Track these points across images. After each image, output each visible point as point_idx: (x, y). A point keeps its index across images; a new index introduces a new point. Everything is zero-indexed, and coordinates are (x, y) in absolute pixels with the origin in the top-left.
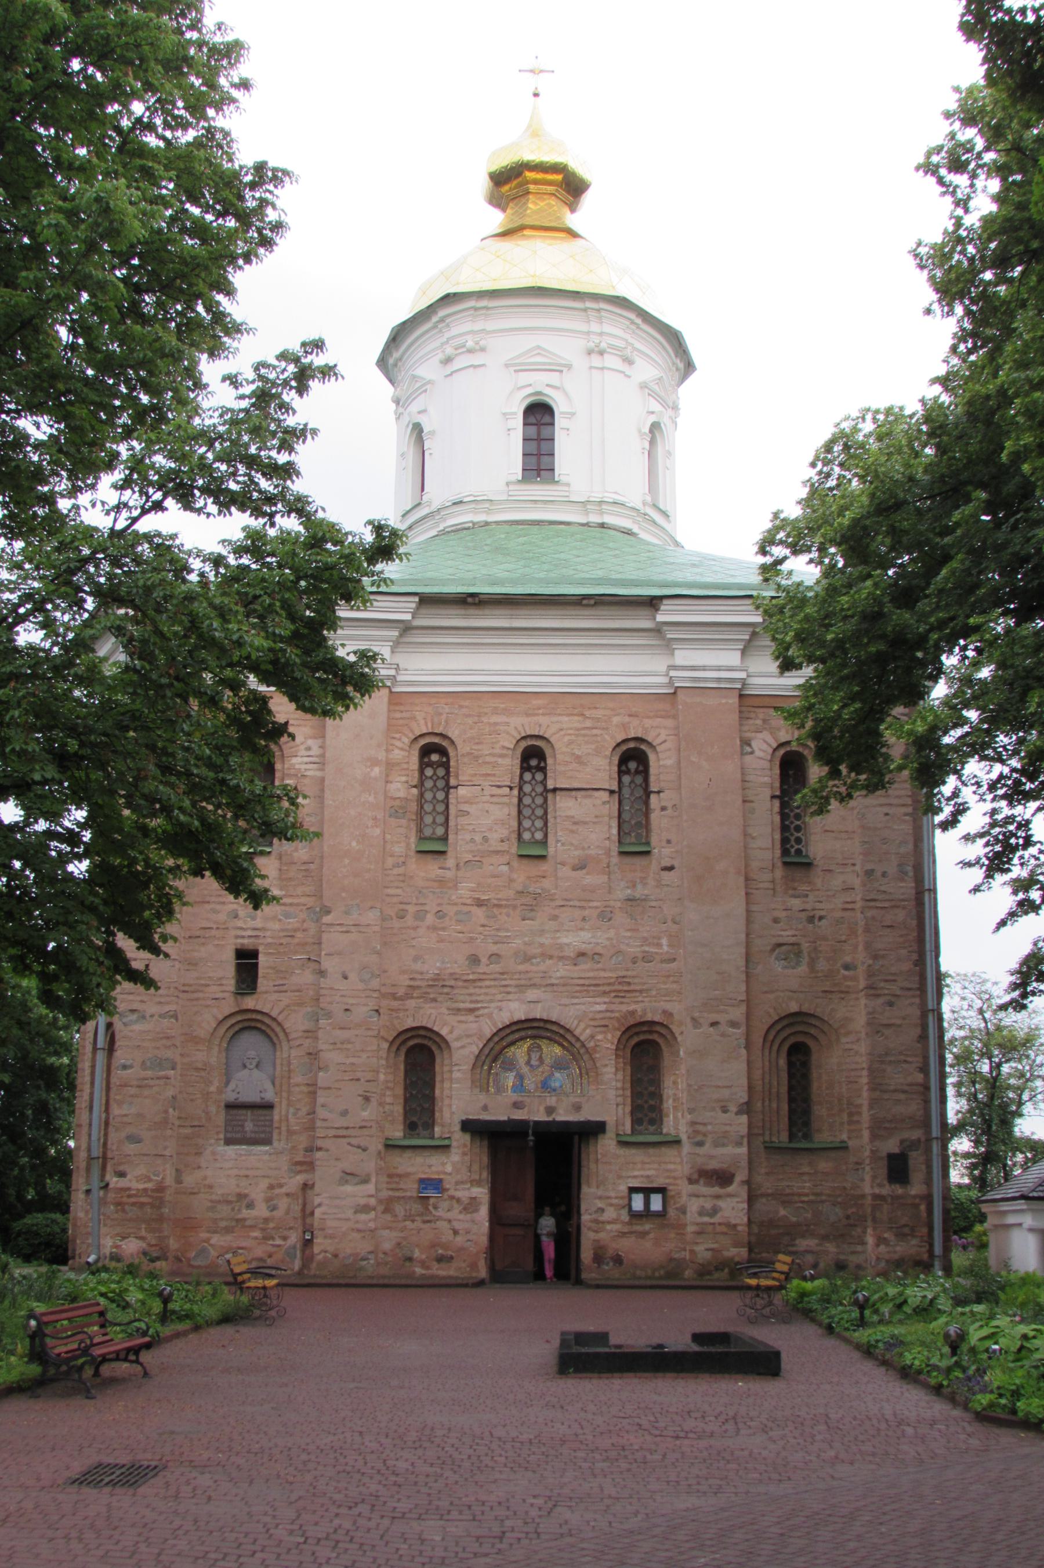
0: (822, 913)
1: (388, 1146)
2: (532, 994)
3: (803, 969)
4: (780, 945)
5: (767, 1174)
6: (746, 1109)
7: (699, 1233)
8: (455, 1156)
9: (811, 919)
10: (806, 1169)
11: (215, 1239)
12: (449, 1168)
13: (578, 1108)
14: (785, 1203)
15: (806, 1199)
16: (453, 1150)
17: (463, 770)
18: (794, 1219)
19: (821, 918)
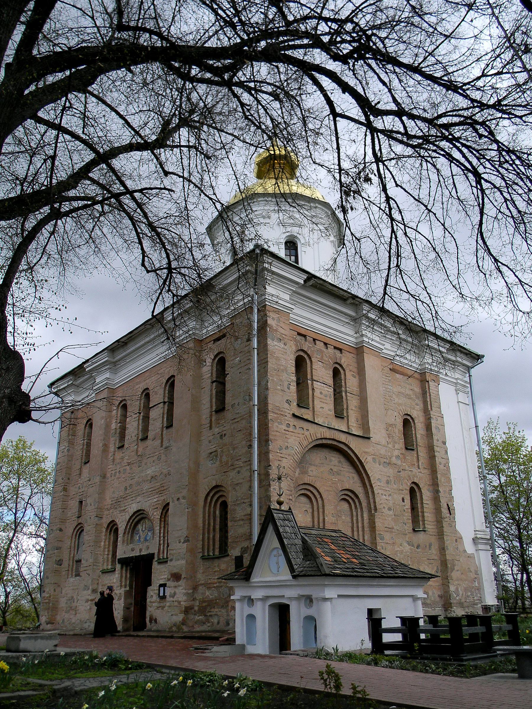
0: (225, 432)
1: (103, 573)
2: (139, 499)
3: (218, 463)
4: (211, 453)
5: (203, 573)
6: (187, 540)
7: (169, 606)
8: (117, 576)
9: (221, 437)
10: (217, 569)
11: (67, 616)
12: (115, 581)
13: (148, 548)
14: (209, 588)
15: (215, 585)
16: (116, 572)
17: (129, 409)
18: (211, 597)
19: (225, 435)
